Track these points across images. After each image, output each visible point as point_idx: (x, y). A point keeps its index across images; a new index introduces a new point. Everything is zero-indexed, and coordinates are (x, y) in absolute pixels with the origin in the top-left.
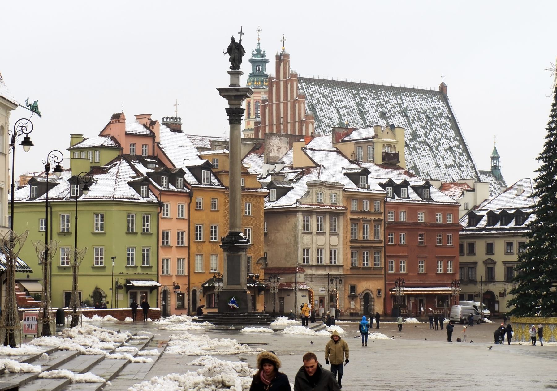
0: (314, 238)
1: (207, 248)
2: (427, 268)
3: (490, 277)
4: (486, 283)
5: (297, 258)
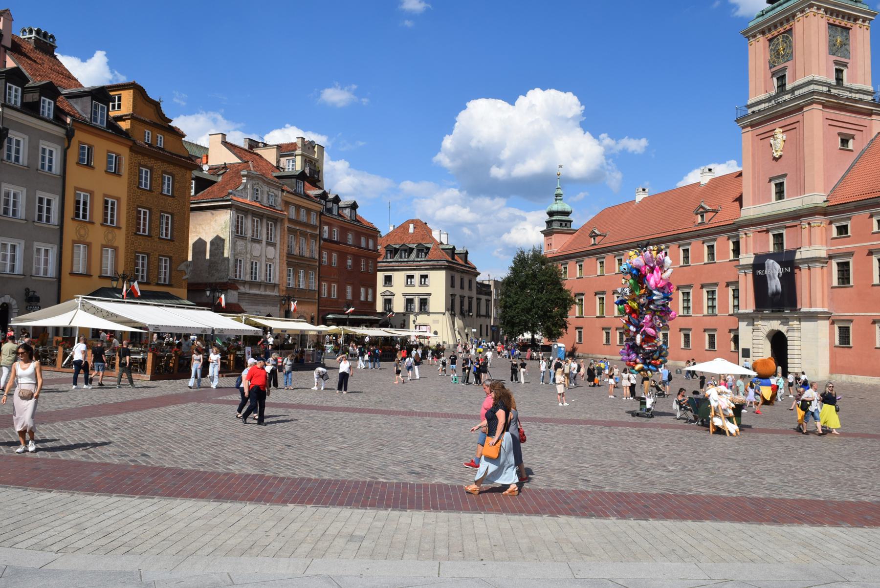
0: (249, 245)
1: (97, 234)
5: (228, 270)
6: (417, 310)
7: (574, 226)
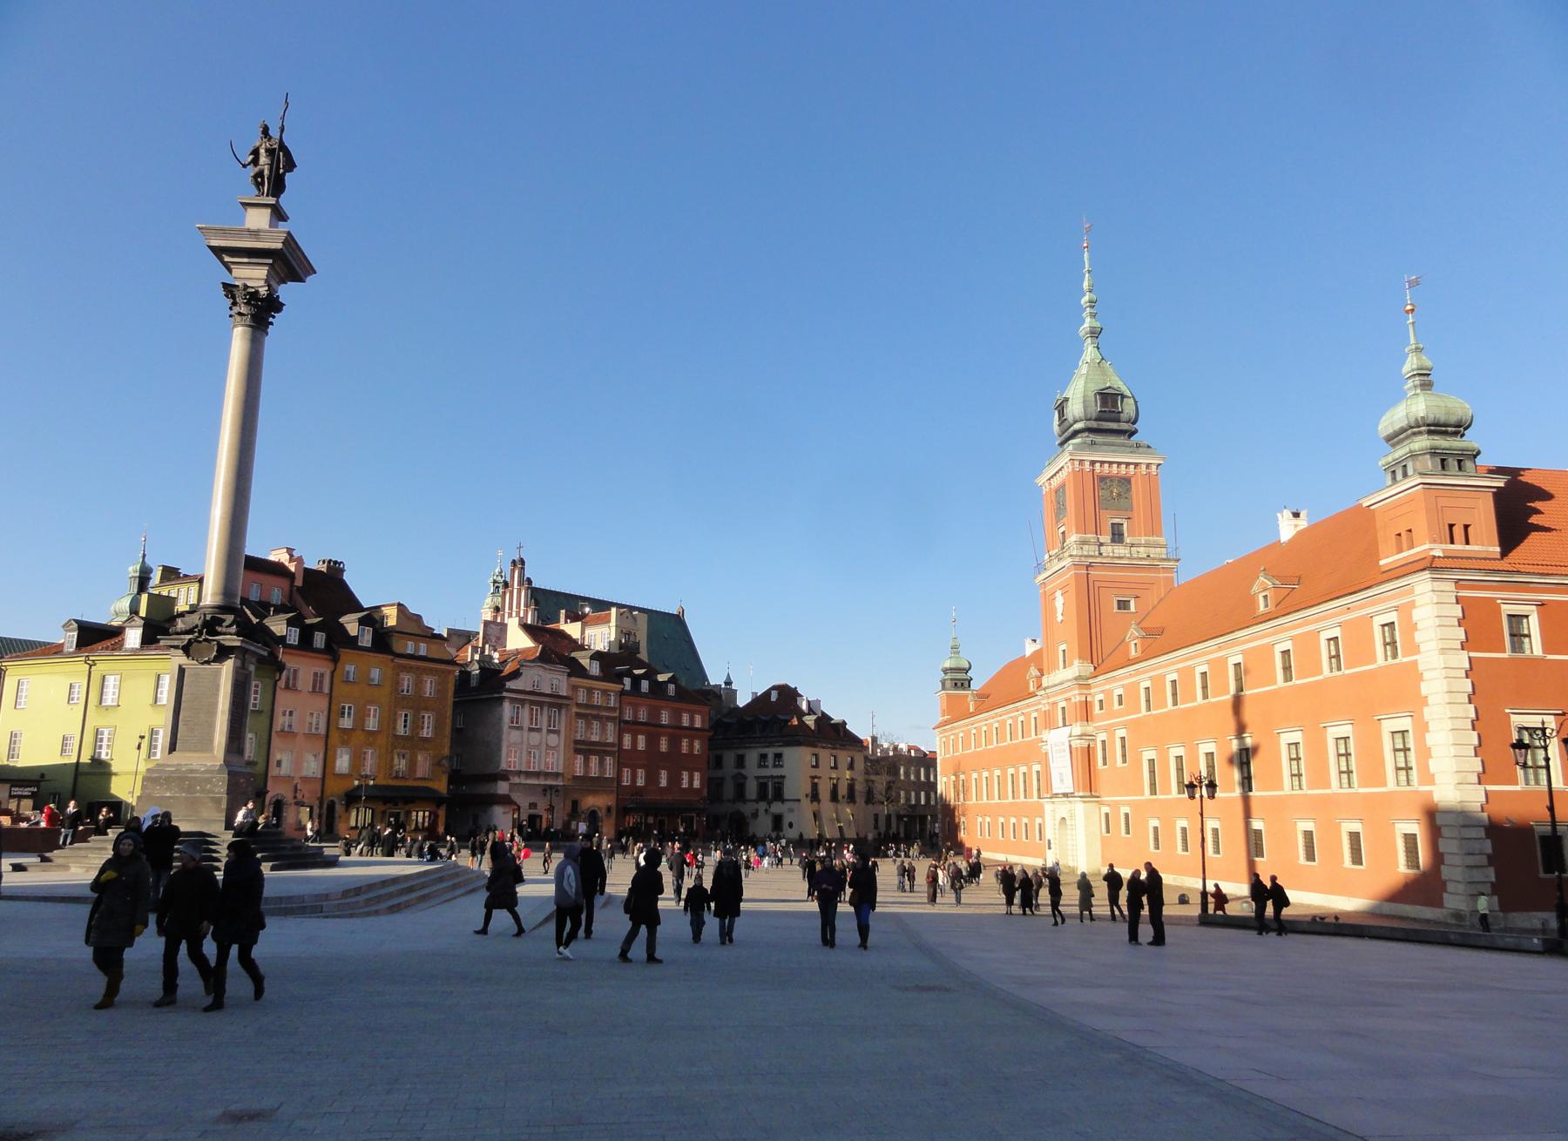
0: (526, 733)
2: (669, 780)
3: (740, 794)
4: (734, 801)
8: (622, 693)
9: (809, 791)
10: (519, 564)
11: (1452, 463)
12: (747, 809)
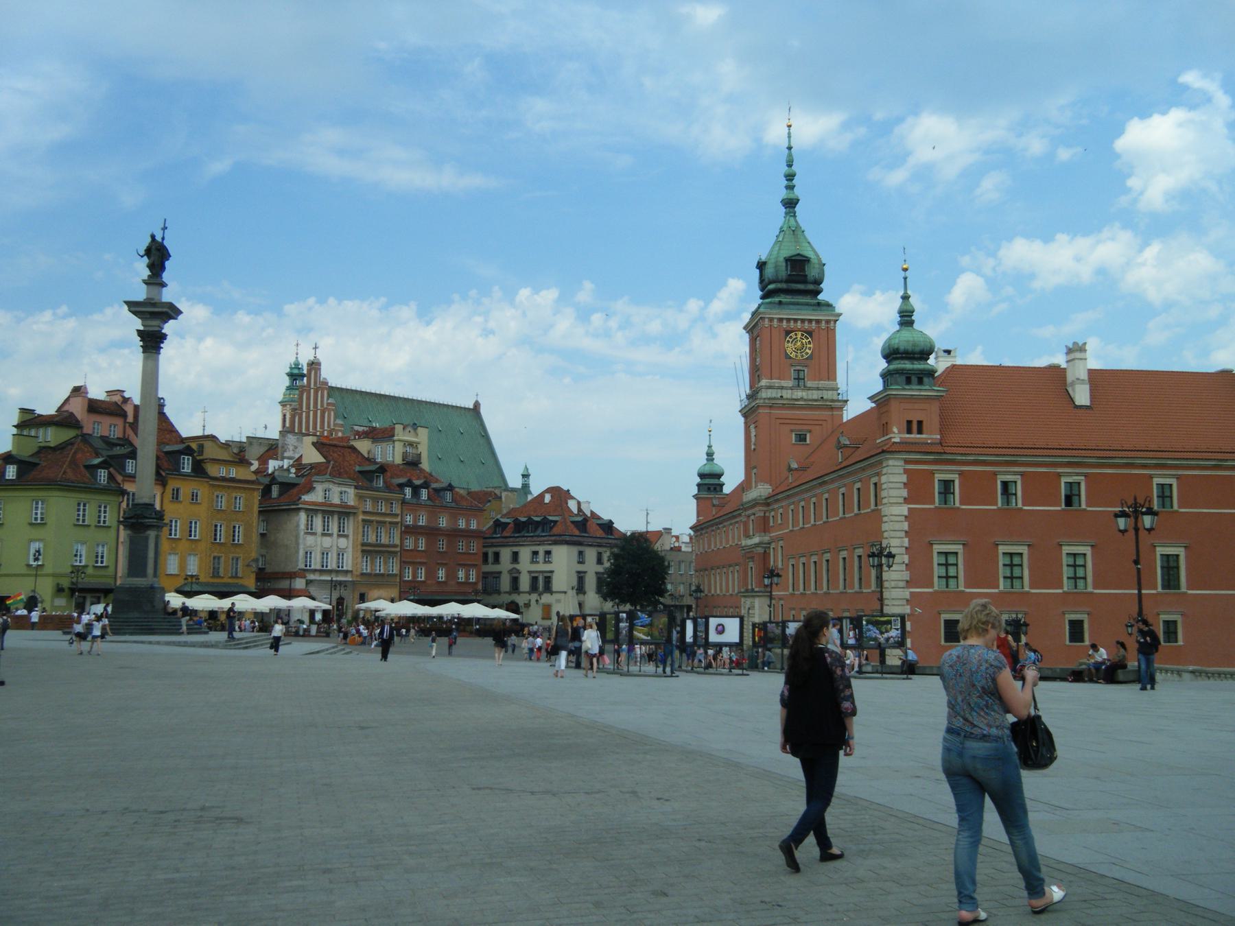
0: (319, 539)
2: (447, 576)
4: (510, 593)
5: (297, 561)
6: (541, 589)
7: (727, 490)
8: (404, 502)
9: (575, 583)
10: (314, 365)
11: (914, 379)
12: (521, 600)
